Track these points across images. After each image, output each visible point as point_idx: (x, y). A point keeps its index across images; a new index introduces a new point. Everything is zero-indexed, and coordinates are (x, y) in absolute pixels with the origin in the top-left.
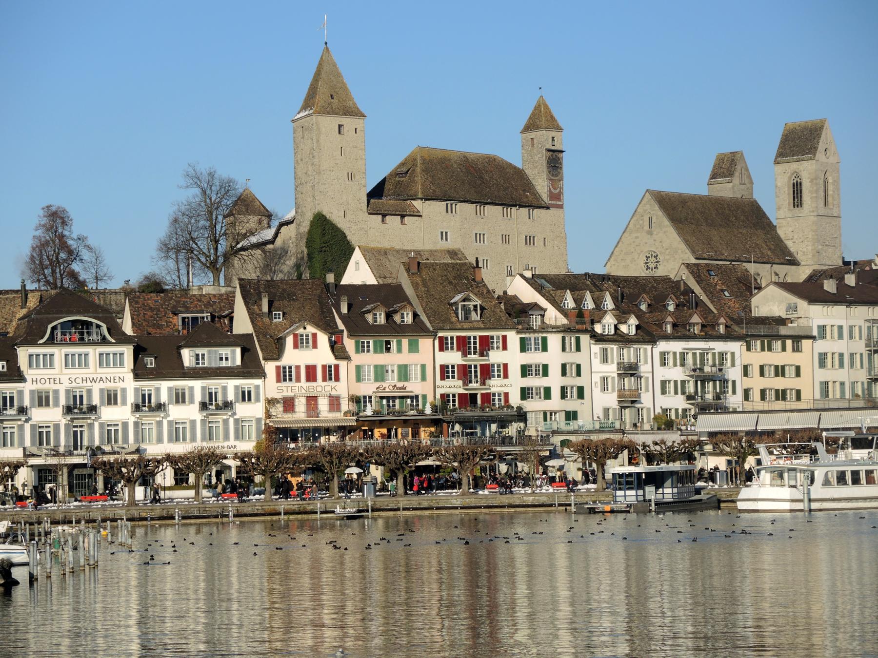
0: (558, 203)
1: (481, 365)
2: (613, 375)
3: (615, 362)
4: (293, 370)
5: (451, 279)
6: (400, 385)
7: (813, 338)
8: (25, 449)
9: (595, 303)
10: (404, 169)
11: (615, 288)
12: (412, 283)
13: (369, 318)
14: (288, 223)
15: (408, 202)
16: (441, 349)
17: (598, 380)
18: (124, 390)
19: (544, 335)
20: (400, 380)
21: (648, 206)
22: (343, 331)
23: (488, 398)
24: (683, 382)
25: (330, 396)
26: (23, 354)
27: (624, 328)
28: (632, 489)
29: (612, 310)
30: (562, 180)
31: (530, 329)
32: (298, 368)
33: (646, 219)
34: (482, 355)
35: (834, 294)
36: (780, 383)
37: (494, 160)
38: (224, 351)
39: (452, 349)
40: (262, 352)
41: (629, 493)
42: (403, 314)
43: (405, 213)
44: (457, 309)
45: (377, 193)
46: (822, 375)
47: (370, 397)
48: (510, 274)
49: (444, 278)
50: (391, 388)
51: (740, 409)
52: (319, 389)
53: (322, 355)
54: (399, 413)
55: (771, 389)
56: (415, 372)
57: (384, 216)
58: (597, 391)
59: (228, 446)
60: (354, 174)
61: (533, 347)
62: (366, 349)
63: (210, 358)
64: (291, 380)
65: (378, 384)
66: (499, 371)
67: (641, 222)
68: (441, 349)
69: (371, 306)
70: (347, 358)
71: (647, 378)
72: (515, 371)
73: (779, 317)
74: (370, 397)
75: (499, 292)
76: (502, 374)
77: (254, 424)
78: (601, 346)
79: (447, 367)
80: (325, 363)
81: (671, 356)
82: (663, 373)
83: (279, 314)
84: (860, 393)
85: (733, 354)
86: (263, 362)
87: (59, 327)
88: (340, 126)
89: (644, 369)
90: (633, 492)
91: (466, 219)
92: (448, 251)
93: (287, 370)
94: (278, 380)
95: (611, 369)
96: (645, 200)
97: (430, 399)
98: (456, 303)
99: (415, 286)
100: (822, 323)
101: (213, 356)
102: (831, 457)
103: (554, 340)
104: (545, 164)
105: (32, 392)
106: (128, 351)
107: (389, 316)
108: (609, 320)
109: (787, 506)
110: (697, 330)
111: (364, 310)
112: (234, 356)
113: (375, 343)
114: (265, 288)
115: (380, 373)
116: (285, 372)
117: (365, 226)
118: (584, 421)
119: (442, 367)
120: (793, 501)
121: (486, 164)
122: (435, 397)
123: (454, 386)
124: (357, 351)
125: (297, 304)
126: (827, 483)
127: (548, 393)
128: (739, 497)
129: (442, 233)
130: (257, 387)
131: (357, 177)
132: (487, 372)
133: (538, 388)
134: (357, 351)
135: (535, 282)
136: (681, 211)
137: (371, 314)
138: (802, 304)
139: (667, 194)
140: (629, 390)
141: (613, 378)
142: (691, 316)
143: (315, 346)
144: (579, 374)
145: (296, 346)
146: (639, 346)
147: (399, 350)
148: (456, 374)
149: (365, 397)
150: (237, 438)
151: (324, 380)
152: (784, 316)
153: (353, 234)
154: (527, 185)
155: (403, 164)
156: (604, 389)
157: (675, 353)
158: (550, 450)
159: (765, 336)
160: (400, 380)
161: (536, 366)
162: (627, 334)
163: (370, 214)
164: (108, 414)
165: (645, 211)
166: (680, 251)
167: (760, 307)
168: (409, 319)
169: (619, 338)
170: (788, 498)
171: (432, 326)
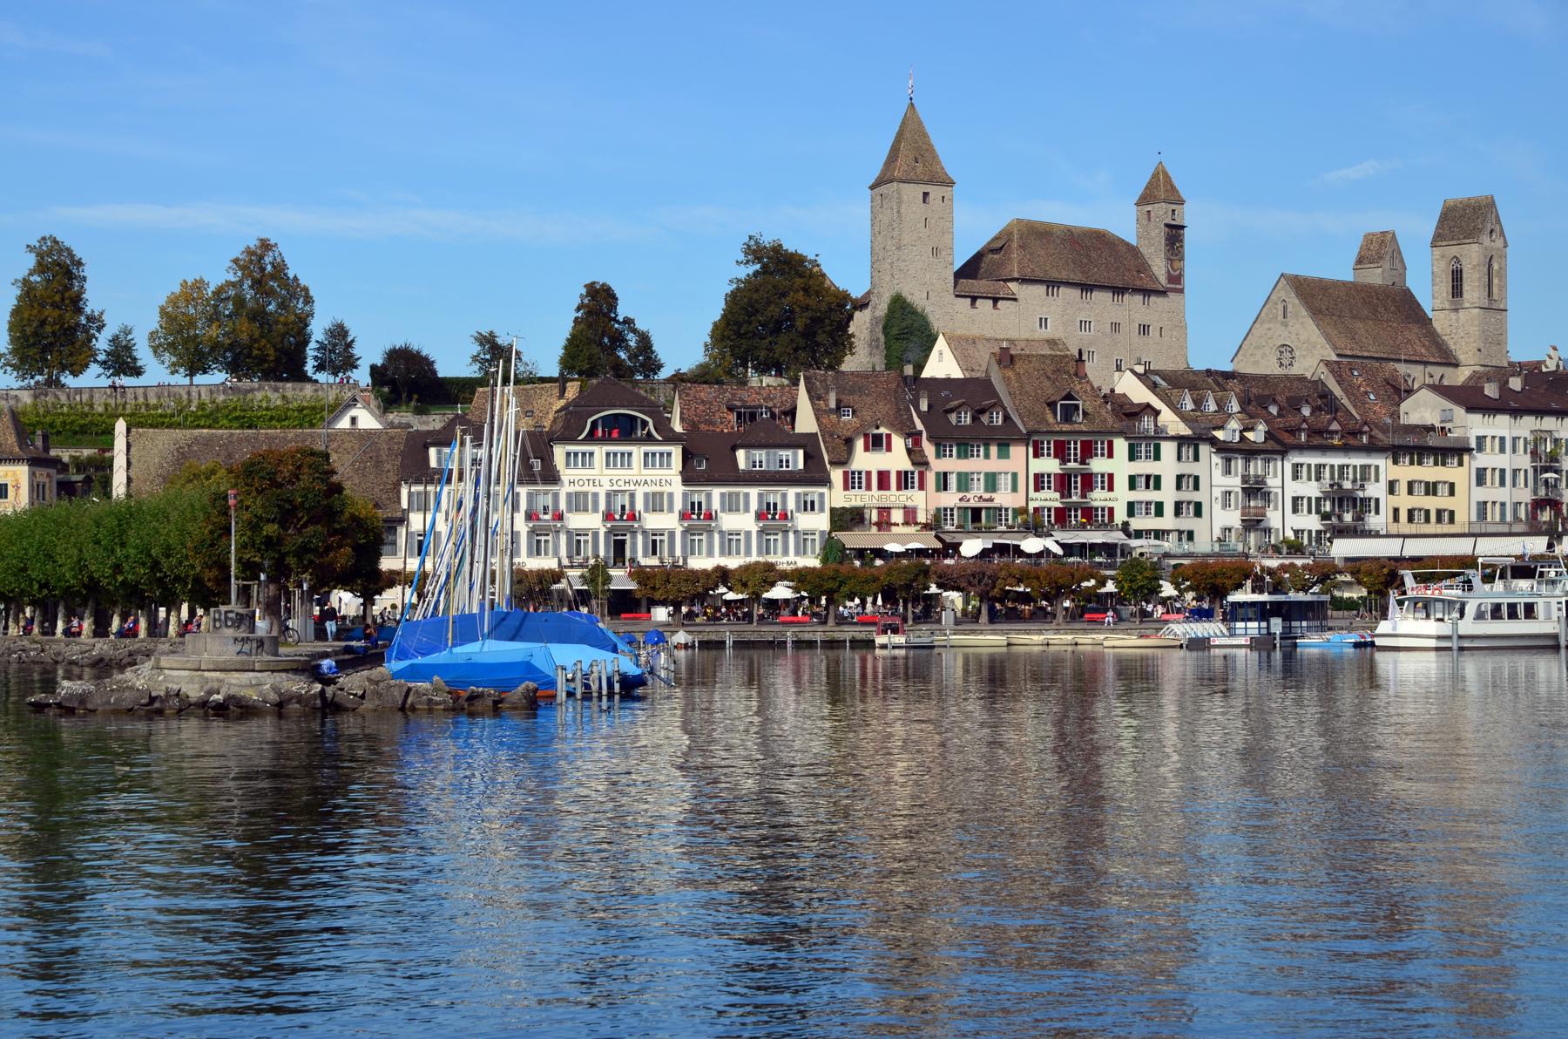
4: (863, 476)
5: (1049, 374)
6: (987, 496)
7: (1469, 450)
8: (560, 561)
9: (1218, 405)
10: (998, 245)
12: (1004, 378)
14: (861, 305)
16: (1036, 455)
17: (1219, 496)
18: (671, 495)
20: (986, 490)
21: (1283, 295)
22: (920, 433)
24: (1319, 500)
25: (905, 508)
26: (559, 452)
27: (1250, 435)
30: (1182, 259)
32: (869, 474)
33: (1280, 307)
34: (1083, 462)
36: (1432, 503)
38: (785, 454)
39: (1049, 455)
41: (1250, 624)
45: (970, 270)
46: (1480, 494)
47: (952, 510)
48: (1119, 369)
51: (1383, 532)
52: (893, 499)
53: (896, 458)
55: (1420, 510)
56: (1004, 482)
57: (974, 299)
61: (1143, 455)
63: (768, 460)
64: (860, 487)
65: (961, 495)
66: (1103, 482)
68: (1036, 455)
70: (926, 464)
71: (1276, 494)
72: (1121, 483)
74: (952, 510)
75: (1105, 390)
77: (817, 537)
79: (1043, 476)
82: (1294, 488)
84: (1523, 516)
85: (1377, 467)
86: (828, 466)
87: (600, 422)
88: (926, 195)
89: (1273, 482)
90: (1255, 624)
92: (1047, 341)
94: (846, 488)
95: (1235, 482)
96: (1280, 285)
99: (1007, 380)
100: (1481, 434)
101: (771, 457)
102: (1487, 587)
103: (1168, 449)
104: (1163, 241)
105: (569, 495)
106: (676, 452)
108: (1234, 425)
109: (1433, 643)
112: (798, 460)
115: (964, 482)
116: (853, 478)
118: (1204, 544)
119: (1036, 476)
120: (1439, 638)
123: (1050, 499)
124: (938, 456)
125: (868, 400)
126: (1480, 616)
132: (1088, 482)
133: (1149, 503)
134: (938, 456)
138: (1459, 412)
139: (1306, 279)
142: (1330, 423)
143: (889, 449)
144: (1196, 487)
145: (867, 449)
147: (987, 456)
149: (945, 509)
150: (797, 553)
151: (899, 488)
152: (1438, 425)
154: (1143, 267)
155: (996, 239)
156: (1226, 504)
159: (1415, 448)
160: (986, 490)
163: (957, 296)
164: (652, 521)
168: (998, 420)
170: (1434, 632)
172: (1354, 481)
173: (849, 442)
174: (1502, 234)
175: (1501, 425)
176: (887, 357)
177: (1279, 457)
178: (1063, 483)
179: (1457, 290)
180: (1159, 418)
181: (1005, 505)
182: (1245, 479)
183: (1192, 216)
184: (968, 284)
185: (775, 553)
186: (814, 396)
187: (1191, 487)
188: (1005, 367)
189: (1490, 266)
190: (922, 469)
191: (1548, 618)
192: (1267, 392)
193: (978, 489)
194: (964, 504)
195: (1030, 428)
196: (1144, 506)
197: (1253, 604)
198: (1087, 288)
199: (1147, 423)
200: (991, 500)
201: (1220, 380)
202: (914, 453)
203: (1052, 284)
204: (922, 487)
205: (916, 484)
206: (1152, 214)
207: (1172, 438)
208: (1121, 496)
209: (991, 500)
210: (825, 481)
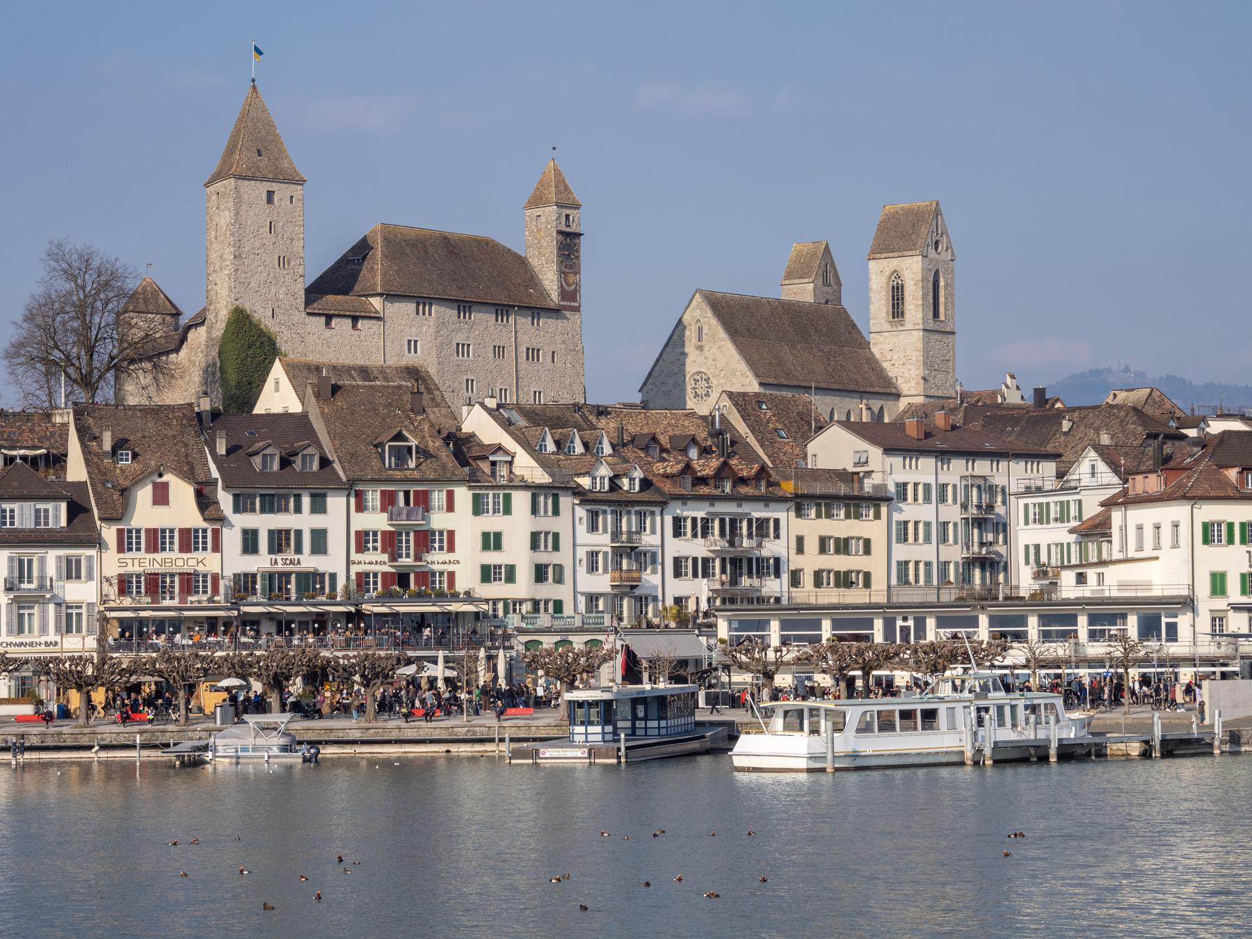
0: (572, 304)
2: (605, 549)
3: (609, 530)
7: (888, 500)
16: (361, 508)
21: (697, 312)
22: (215, 482)
24: (706, 561)
29: (609, 456)
30: (577, 273)
40: (98, 509)
41: (591, 729)
43: (358, 314)
46: (901, 552)
52: (180, 563)
55: (829, 572)
57: (329, 318)
59: (46, 643)
60: (288, 260)
64: (138, 549)
66: (441, 541)
69: (261, 444)
70: (222, 519)
73: (844, 469)
75: (448, 426)
77: (84, 611)
79: (367, 533)
80: (188, 526)
82: (676, 547)
83: (127, 454)
84: (952, 578)
85: (777, 521)
86: (98, 523)
88: (270, 194)
90: (598, 729)
91: (444, 323)
94: (120, 549)
95: (603, 541)
96: (694, 303)
97: (341, 582)
111: (250, 450)
112: (58, 514)
116: (130, 538)
119: (358, 533)
123: (376, 562)
124: (237, 509)
129: (409, 341)
130: (90, 558)
131: (293, 263)
132: (425, 540)
134: (237, 509)
138: (875, 453)
141: (606, 554)
144: (556, 547)
147: (298, 510)
152: (851, 469)
153: (286, 342)
154: (532, 280)
156: (593, 568)
162: (628, 492)
163: (309, 314)
166: (739, 374)
172: (750, 536)
173: (125, 492)
175: (924, 471)
177: (657, 510)
178: (391, 542)
181: (321, 570)
182: (616, 535)
185: (30, 631)
186: (85, 434)
190: (217, 526)
192: (645, 431)
195: (351, 474)
198: (464, 306)
202: (205, 501)
203: (423, 301)
204: (217, 548)
205: (209, 545)
207: (527, 487)
210: (96, 542)
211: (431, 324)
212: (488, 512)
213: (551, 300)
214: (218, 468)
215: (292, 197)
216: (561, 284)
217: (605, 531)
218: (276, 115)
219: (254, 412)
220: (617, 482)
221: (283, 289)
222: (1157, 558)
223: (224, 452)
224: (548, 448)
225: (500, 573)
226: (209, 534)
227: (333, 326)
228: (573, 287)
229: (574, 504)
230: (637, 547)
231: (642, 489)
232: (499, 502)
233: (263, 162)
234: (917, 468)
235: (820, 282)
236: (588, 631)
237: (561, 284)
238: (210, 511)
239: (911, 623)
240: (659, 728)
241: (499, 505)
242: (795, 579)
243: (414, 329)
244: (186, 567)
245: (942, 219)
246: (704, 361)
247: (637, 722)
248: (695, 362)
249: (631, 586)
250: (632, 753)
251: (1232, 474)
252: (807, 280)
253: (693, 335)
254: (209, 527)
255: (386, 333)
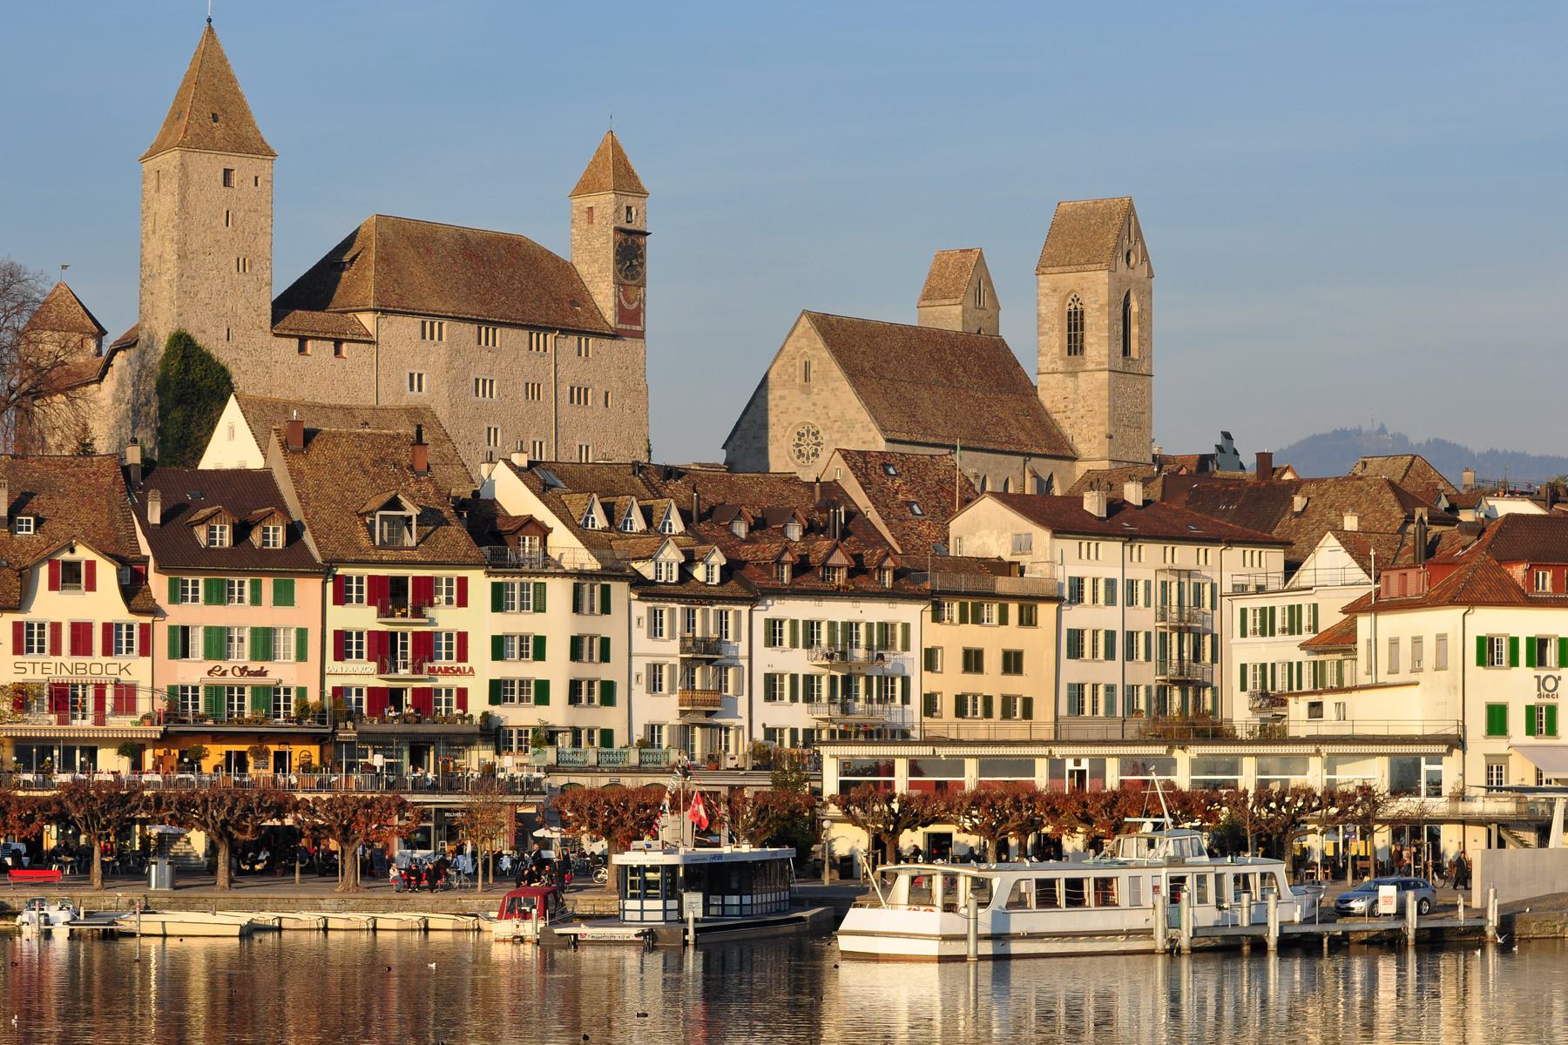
0: (634, 328)
1: (414, 634)
4: (47, 630)
6: (255, 666)
7: (1058, 600)
11: (689, 492)
12: (291, 471)
13: (201, 534)
15: (350, 315)
16: (342, 598)
19: (541, 580)
20: (254, 657)
21: (804, 341)
23: (425, 699)
24: (809, 679)
28: (654, 897)
29: (680, 534)
31: (517, 568)
32: (56, 627)
33: (799, 363)
35: (1101, 519)
37: (519, 244)
39: (360, 600)
41: (648, 904)
42: (268, 530)
43: (343, 337)
44: (373, 522)
46: (1074, 671)
48: (491, 460)
49: (353, 462)
50: (237, 672)
52: (96, 669)
54: (249, 721)
56: (286, 643)
57: (303, 341)
58: (640, 690)
60: (250, 262)
62: (190, 595)
65: (211, 664)
66: (449, 646)
67: (791, 370)
69: (207, 511)
70: (155, 611)
72: (480, 649)
73: (999, 558)
74: (195, 689)
76: (455, 651)
78: (650, 604)
79: (349, 635)
80: (109, 620)
81: (786, 627)
82: (768, 660)
83: (28, 522)
84: (1142, 706)
85: (906, 627)
88: (227, 172)
90: (659, 904)
93: (36, 630)
95: (669, 650)
96: (800, 329)
98: (371, 513)
99: (296, 476)
104: (612, 256)
107: (241, 532)
108: (672, 555)
109: (933, 948)
110: (840, 577)
111: (193, 519)
113: (208, 584)
114: (7, 469)
115: (219, 643)
117: (267, 359)
119: (336, 632)
120: (945, 938)
121: (503, 252)
122: (322, 694)
123: (361, 674)
124: (173, 599)
125: (63, 504)
127: (542, 693)
128: (843, 927)
129: (412, 375)
131: (256, 267)
132: (426, 646)
134: (173, 599)
135: (536, 475)
136: (864, 353)
137: (205, 526)
138: (1041, 536)
139: (840, 320)
140: (702, 691)
141: (672, 667)
142: (830, 554)
143: (91, 586)
144: (605, 657)
145: (53, 586)
146: (726, 607)
147: (256, 600)
148: (365, 650)
149: (185, 689)
151: (107, 651)
152: (1007, 558)
153: (245, 373)
154: (579, 296)
156: (655, 686)
157: (794, 623)
158: (538, 804)
159: (968, 594)
160: (254, 657)
161: (521, 638)
162: (704, 584)
163: (276, 335)
165: (798, 349)
167: (964, 539)
168: (279, 539)
169: (685, 591)
171: (322, 555)
172: (869, 647)
174: (1145, 257)
176: (160, 431)
178: (383, 648)
179: (1075, 345)
180: (550, 538)
181: (286, 683)
183: (653, 218)
184: (300, 318)
187: (596, 656)
188: (294, 452)
189: (1126, 305)
190: (147, 620)
191: (1136, 904)
193: (242, 655)
194: (216, 680)
196: (516, 688)
197: (654, 869)
199: (530, 544)
200: (262, 673)
201: (655, 479)
202: (132, 588)
204: (145, 650)
206: (596, 212)
207: (566, 574)
208: (482, 669)
209: (262, 673)
211: (442, 352)
212: (513, 609)
213: (605, 322)
214: (149, 543)
215: (256, 178)
216: (620, 301)
217: (672, 636)
218: (238, 69)
219: (200, 467)
220: (689, 569)
221: (243, 301)
222: (1417, 684)
223: (158, 521)
224: (596, 523)
225: (529, 692)
226: (136, 632)
227: (309, 352)
228: (635, 305)
229: (630, 600)
230: (716, 659)
231: (723, 580)
232: (528, 595)
233: (219, 129)
234: (1097, 558)
235: (971, 305)
236: (647, 771)
237: (620, 301)
238: (138, 601)
239: (1085, 765)
240: (741, 905)
241: (528, 599)
242: (930, 704)
243: (418, 359)
244: (104, 674)
245: (1136, 218)
246: (812, 408)
247: (711, 897)
248: (799, 409)
249: (707, 712)
250: (704, 939)
251: (1518, 572)
252: (953, 301)
253: (797, 373)
254: (138, 620)
255: (380, 363)
